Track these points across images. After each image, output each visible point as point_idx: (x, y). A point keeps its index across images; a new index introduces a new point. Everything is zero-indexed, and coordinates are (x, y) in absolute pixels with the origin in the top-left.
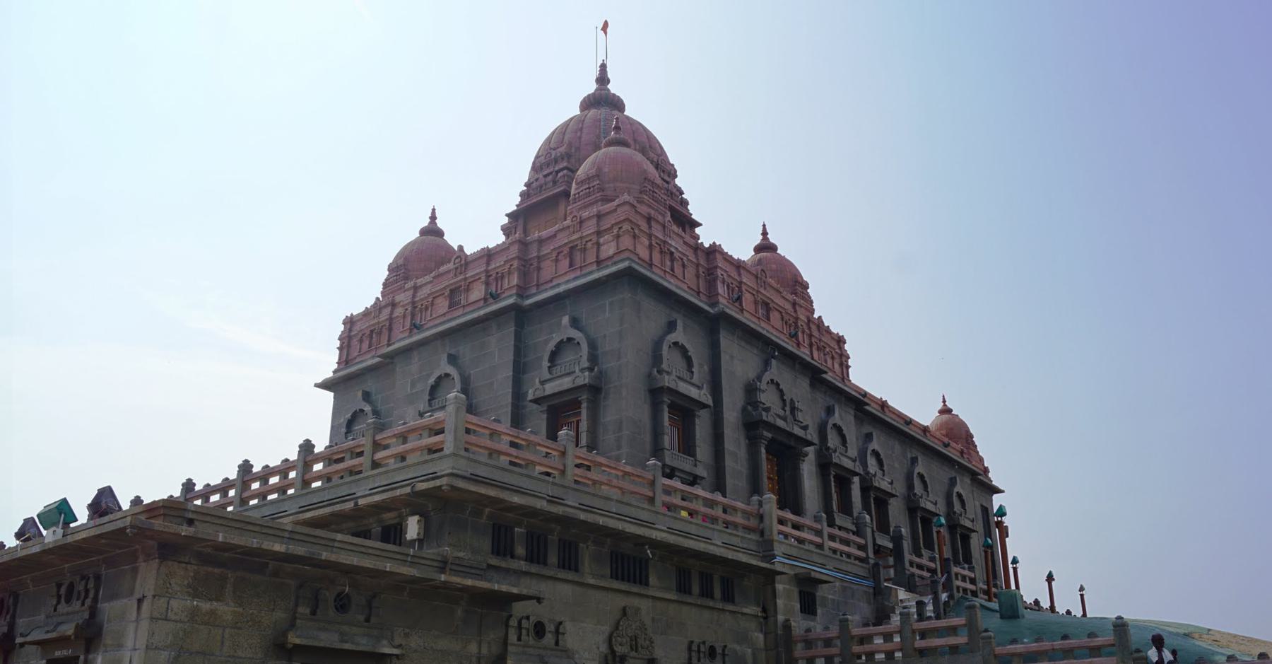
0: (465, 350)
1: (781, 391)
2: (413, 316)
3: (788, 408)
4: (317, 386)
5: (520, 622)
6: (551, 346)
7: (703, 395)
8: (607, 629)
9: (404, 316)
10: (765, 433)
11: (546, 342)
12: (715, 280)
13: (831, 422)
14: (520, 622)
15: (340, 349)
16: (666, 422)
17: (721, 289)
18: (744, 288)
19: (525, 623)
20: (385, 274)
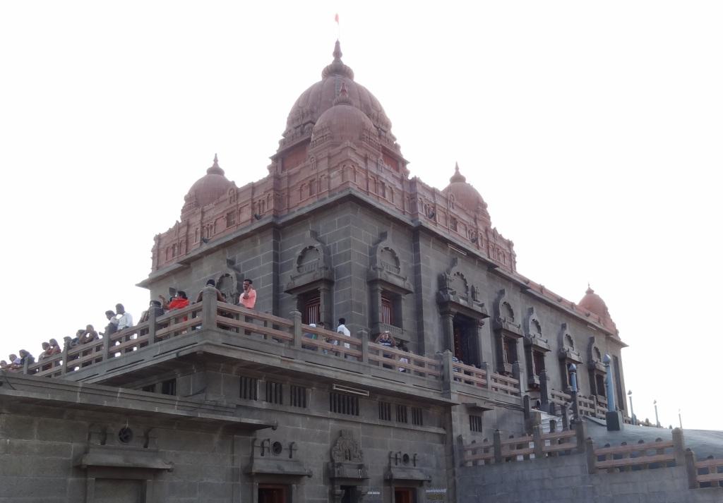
0: (238, 255)
1: (465, 280)
2: (202, 233)
3: (469, 292)
4: (139, 285)
5: (263, 443)
6: (299, 253)
7: (407, 284)
8: (328, 445)
10: (452, 310)
11: (295, 250)
12: (415, 204)
13: (501, 302)
14: (263, 443)
15: (153, 258)
16: (380, 304)
17: (420, 209)
18: (437, 206)
19: (267, 444)
20: (182, 203)
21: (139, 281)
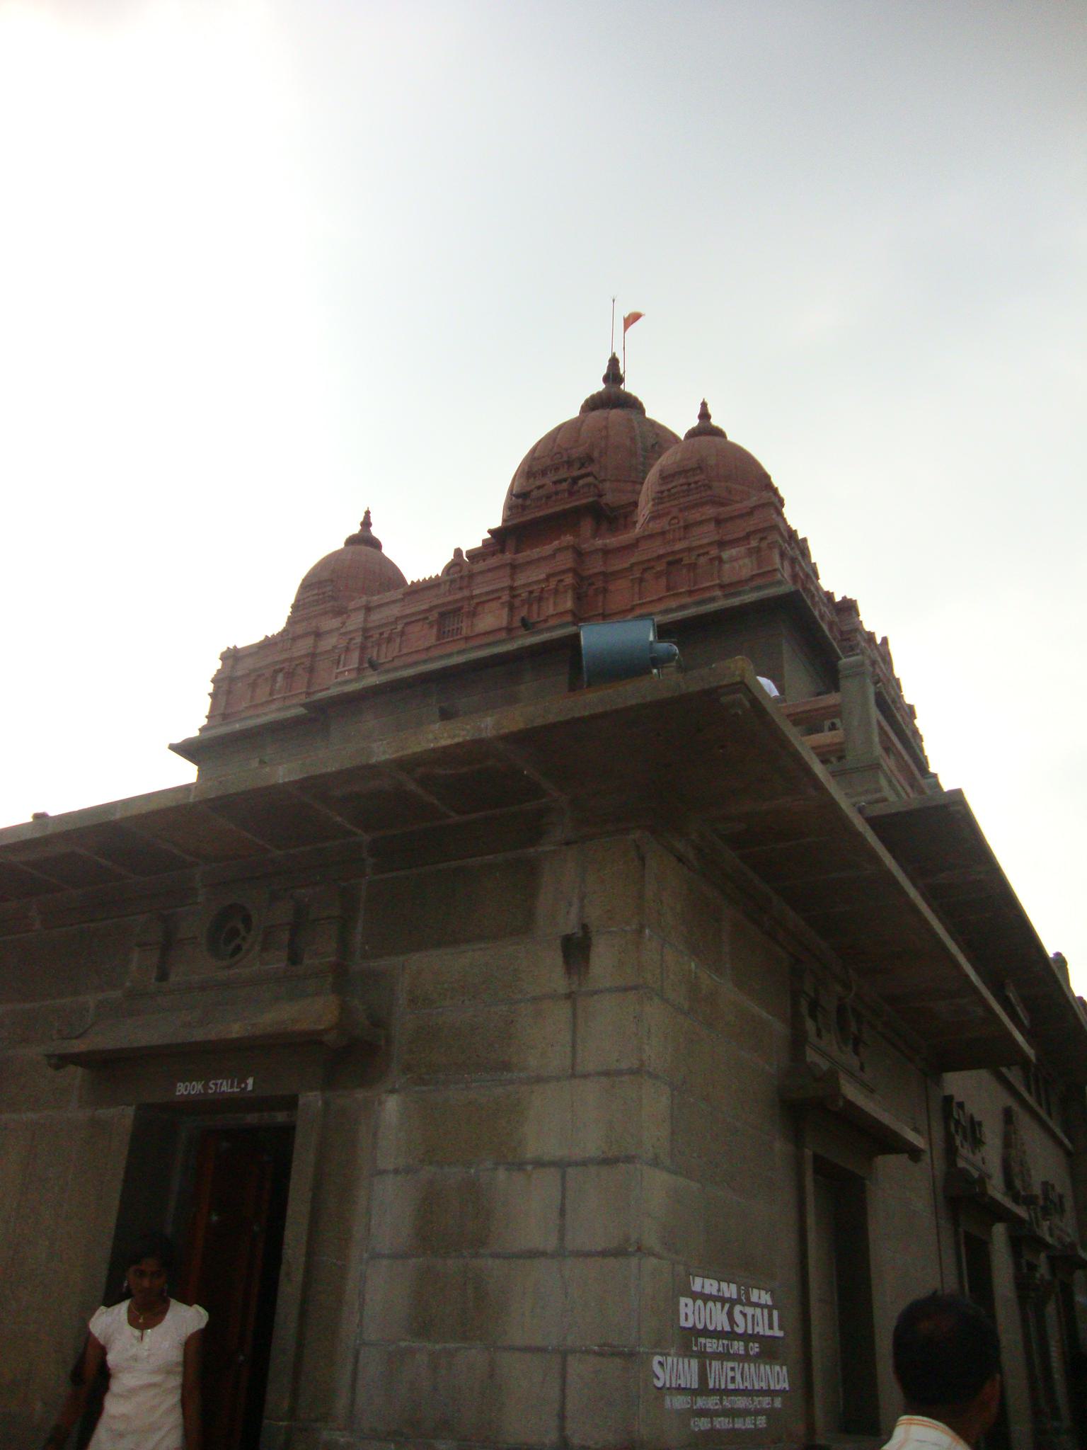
2: (363, 648)
4: (175, 748)
9: (347, 650)
21: (178, 740)
